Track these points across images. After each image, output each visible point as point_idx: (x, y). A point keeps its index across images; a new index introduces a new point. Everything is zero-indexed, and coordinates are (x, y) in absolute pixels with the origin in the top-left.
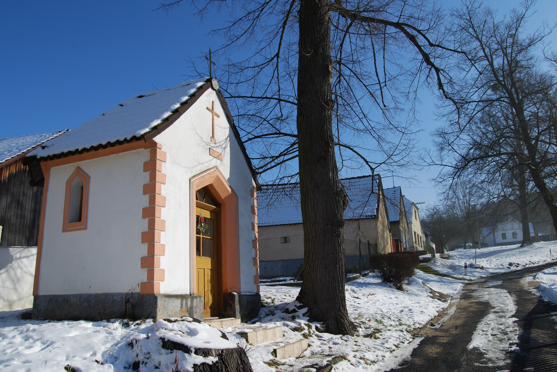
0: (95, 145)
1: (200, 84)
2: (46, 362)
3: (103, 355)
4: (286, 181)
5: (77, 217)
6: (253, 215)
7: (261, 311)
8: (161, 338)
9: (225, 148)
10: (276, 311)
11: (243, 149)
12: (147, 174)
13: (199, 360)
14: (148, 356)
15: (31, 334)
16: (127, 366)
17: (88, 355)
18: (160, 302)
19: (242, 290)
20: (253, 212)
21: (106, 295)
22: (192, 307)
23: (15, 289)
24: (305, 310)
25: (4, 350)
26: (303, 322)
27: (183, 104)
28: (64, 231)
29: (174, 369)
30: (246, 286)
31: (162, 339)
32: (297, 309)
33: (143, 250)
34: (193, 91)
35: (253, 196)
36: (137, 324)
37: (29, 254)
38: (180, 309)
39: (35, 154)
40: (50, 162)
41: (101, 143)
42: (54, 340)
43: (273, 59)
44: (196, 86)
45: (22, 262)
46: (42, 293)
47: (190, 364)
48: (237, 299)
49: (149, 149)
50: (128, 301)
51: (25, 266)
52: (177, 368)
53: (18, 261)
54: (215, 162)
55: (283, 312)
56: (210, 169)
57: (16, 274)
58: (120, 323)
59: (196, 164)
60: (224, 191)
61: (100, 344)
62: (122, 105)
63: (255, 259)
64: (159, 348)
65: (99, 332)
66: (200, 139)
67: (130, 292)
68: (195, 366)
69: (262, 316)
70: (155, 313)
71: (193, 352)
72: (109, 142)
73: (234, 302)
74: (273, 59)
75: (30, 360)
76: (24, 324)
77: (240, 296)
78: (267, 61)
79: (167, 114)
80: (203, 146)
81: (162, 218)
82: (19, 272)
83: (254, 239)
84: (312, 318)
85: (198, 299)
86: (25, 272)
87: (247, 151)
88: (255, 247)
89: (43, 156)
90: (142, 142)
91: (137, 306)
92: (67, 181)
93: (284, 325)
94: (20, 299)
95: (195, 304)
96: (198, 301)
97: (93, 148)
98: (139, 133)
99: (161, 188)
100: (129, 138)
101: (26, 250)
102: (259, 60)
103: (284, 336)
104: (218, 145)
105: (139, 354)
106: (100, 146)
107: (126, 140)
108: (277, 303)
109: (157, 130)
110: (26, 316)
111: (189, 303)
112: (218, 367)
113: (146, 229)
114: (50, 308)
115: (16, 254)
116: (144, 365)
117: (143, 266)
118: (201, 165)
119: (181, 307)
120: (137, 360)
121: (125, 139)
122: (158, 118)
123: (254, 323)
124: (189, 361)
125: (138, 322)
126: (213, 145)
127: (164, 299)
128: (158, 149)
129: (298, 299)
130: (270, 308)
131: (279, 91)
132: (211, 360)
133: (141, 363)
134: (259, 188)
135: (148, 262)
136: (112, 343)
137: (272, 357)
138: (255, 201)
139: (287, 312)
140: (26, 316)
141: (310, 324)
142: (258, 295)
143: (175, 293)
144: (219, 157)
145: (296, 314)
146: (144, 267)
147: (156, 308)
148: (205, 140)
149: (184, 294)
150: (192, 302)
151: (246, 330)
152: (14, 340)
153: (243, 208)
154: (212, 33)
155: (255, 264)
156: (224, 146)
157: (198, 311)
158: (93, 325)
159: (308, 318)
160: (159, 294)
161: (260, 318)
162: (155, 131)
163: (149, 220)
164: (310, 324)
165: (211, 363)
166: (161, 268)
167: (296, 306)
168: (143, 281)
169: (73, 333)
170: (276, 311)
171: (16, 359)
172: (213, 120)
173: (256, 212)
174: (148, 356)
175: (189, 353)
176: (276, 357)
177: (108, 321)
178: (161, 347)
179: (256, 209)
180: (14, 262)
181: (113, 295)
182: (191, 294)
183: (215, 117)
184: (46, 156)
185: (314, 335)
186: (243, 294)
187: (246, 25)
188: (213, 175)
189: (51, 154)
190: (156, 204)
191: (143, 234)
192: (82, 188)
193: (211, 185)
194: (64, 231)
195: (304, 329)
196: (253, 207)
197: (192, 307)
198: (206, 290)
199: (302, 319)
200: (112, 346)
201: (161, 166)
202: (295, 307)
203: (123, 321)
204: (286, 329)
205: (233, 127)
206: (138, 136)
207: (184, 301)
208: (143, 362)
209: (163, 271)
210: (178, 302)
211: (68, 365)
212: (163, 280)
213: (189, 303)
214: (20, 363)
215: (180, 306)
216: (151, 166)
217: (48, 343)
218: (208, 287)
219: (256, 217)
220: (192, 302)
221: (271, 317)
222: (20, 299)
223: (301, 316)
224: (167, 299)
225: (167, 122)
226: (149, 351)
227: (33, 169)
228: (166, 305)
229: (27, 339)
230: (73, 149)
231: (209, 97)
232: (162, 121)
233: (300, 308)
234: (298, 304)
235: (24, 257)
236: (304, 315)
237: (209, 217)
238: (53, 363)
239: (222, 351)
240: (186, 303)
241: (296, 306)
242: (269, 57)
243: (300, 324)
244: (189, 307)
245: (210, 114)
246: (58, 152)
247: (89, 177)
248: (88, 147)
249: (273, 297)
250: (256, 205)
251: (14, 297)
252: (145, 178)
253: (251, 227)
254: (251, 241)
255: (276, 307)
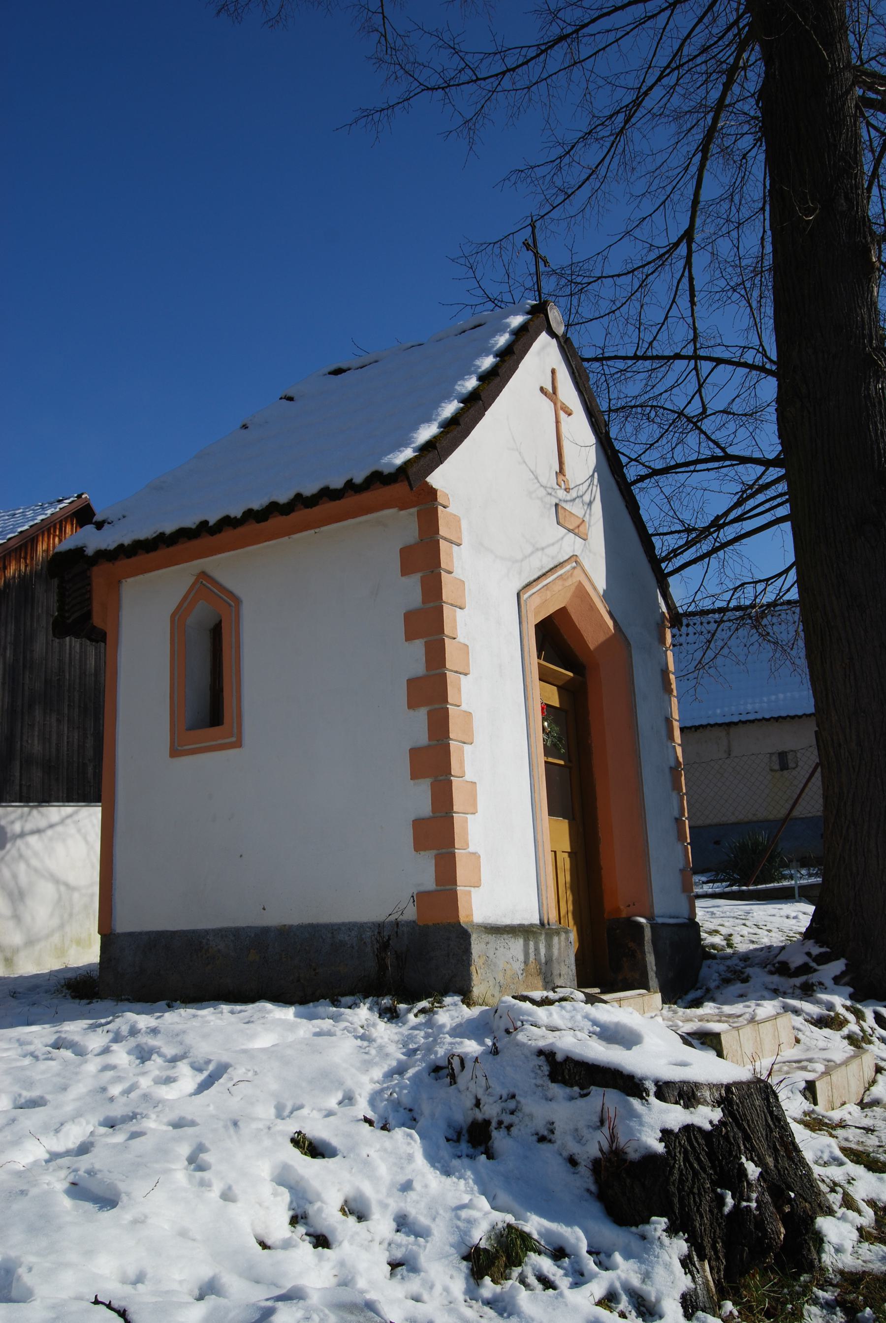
0: (257, 504)
1: (516, 321)
2: (235, 1124)
3: (372, 1102)
4: (746, 597)
5: (209, 708)
6: (666, 697)
7: (704, 971)
8: (540, 1052)
9: (590, 504)
10: (749, 971)
11: (633, 507)
12: (414, 582)
13: (675, 1116)
14: (512, 1104)
15: (152, 1042)
16: (451, 1134)
17: (332, 1102)
18: (477, 947)
19: (657, 910)
20: (667, 689)
21: (314, 931)
22: (549, 961)
23: (17, 917)
24: (837, 966)
25: (104, 1089)
26: (839, 1002)
27: (484, 378)
28: (175, 752)
29: (606, 1146)
30: (665, 903)
31: (547, 1055)
32: (813, 965)
33: (419, 799)
34: (502, 340)
35: (662, 640)
36: (423, 1011)
37: (43, 823)
38: (522, 966)
39: (80, 544)
40: (123, 563)
41: (274, 498)
42: (225, 1058)
43: (676, 245)
44: (508, 325)
45: (27, 845)
46: (122, 925)
47: (652, 1128)
48: (648, 934)
49: (414, 510)
50: (385, 946)
51: (36, 854)
52: (613, 1138)
53: (19, 842)
54: (570, 545)
55: (771, 973)
56: (560, 565)
57: (15, 876)
58: (370, 1009)
59: (529, 549)
60: (597, 626)
61: (353, 1071)
62: (290, 399)
63: (678, 821)
64: (539, 1082)
65: (330, 1034)
66: (532, 476)
67: (392, 918)
68: (666, 1134)
69: (712, 985)
70: (468, 978)
71: (652, 1093)
72: (299, 496)
73: (641, 943)
74: (676, 245)
75: (189, 1117)
76: (115, 1015)
77: (654, 927)
78: (652, 256)
79: (450, 409)
80: (541, 499)
81: (464, 707)
82: (22, 867)
83: (672, 763)
84: (863, 991)
85: (563, 936)
86: (36, 870)
87: (642, 512)
88: (677, 786)
89: (103, 546)
90: (399, 489)
91: (409, 960)
92: (173, 616)
93: (786, 1008)
94: (30, 943)
95: (555, 952)
96: (563, 944)
97: (250, 515)
98: (390, 464)
99: (455, 620)
100: (359, 479)
101: (35, 812)
102: (631, 252)
103: (798, 1041)
104: (574, 494)
105: (484, 1099)
106: (274, 509)
107: (350, 486)
108: (743, 947)
109: (435, 452)
110: (81, 991)
111: (543, 951)
112: (726, 1138)
113: (422, 738)
114: (148, 968)
115: (13, 822)
116: (503, 1131)
117: (420, 844)
118: (539, 553)
119: (526, 962)
120: (480, 1116)
121: (350, 484)
122: (428, 420)
123: (697, 1003)
124: (646, 1119)
125: (424, 1004)
126: (561, 494)
127: (486, 937)
128: (440, 508)
129: (808, 934)
130: (729, 962)
131: (695, 340)
132: (706, 1116)
133: (494, 1124)
134: (677, 619)
135: (437, 833)
136: (386, 1068)
137: (807, 1106)
138: (670, 654)
139: (780, 973)
140: (81, 991)
141: (859, 1006)
142: (693, 927)
143: (507, 921)
144: (578, 530)
145: (814, 978)
146: (425, 849)
147: (470, 965)
148: (543, 480)
149: (526, 922)
150: (549, 946)
151: (716, 1027)
152: (112, 1059)
153: (644, 679)
154: (513, 179)
155: (681, 837)
156: (587, 498)
157: (564, 970)
158: (297, 1015)
159: (851, 990)
160: (473, 925)
161: (708, 990)
162: (431, 455)
163: (429, 713)
164: (859, 1006)
165: (708, 1127)
166: (471, 849)
167: (809, 954)
168: (422, 889)
169: (264, 1041)
170: (749, 971)
171: (153, 1116)
172: (557, 422)
173: (674, 686)
174: (512, 1104)
175: (642, 1098)
176: (815, 1103)
177: (335, 1003)
178: (546, 1079)
179: (672, 677)
180: (8, 846)
181: (333, 929)
182: (542, 924)
183: (562, 415)
184: (112, 547)
185: (874, 1039)
186: (660, 920)
187: (591, 155)
188: (569, 582)
189: (127, 541)
190: (448, 665)
191: (414, 752)
192: (216, 632)
193: (563, 611)
194: (175, 752)
195: (846, 1021)
196: (665, 672)
197: (549, 961)
198: (563, 912)
199: (832, 993)
200: (389, 1075)
201: (450, 555)
202: (806, 959)
203: (377, 1003)
204: (798, 1021)
205: (605, 443)
206: (386, 471)
207: (531, 944)
208: (500, 1123)
209: (476, 856)
210: (516, 946)
211: (299, 1133)
212: (478, 886)
213: (543, 951)
214: (165, 1128)
215: (521, 958)
216: (424, 558)
217: (211, 1067)
218: (567, 906)
219: (674, 701)
220: (549, 946)
221: (738, 987)
222: (30, 943)
223: (829, 983)
224: (491, 938)
225: (456, 430)
226: (512, 1090)
227: (71, 587)
228: (491, 955)
229: (143, 1055)
230: (190, 521)
231: (543, 357)
232: (440, 426)
233: (822, 959)
234: (816, 950)
235: (33, 832)
236: (837, 980)
237: (558, 706)
238: (254, 1125)
239: (728, 1087)
240: (537, 950)
241: (809, 954)
242: (662, 242)
243: (830, 1007)
244: (543, 960)
245: (547, 405)
246: (145, 533)
247: (237, 601)
248: (236, 512)
249: (724, 931)
250: (671, 667)
251: (16, 938)
252: (409, 592)
253: (664, 733)
254: (667, 770)
255: (746, 958)
